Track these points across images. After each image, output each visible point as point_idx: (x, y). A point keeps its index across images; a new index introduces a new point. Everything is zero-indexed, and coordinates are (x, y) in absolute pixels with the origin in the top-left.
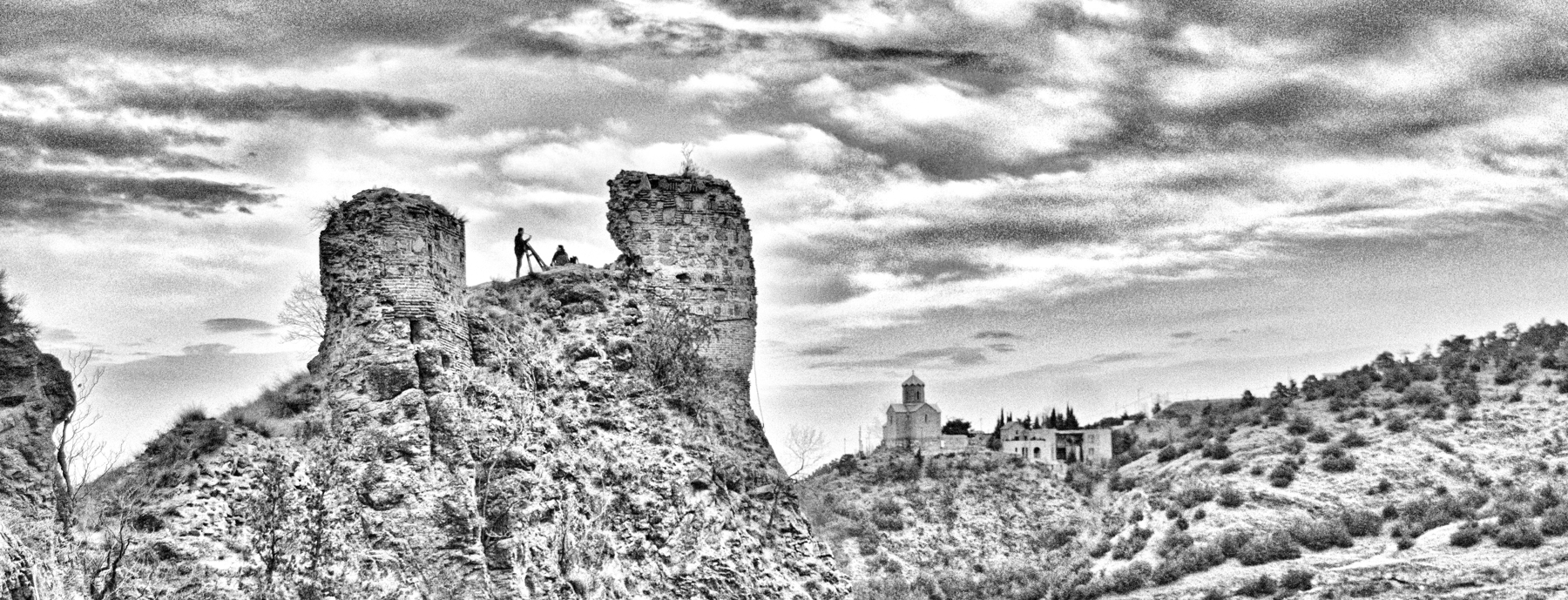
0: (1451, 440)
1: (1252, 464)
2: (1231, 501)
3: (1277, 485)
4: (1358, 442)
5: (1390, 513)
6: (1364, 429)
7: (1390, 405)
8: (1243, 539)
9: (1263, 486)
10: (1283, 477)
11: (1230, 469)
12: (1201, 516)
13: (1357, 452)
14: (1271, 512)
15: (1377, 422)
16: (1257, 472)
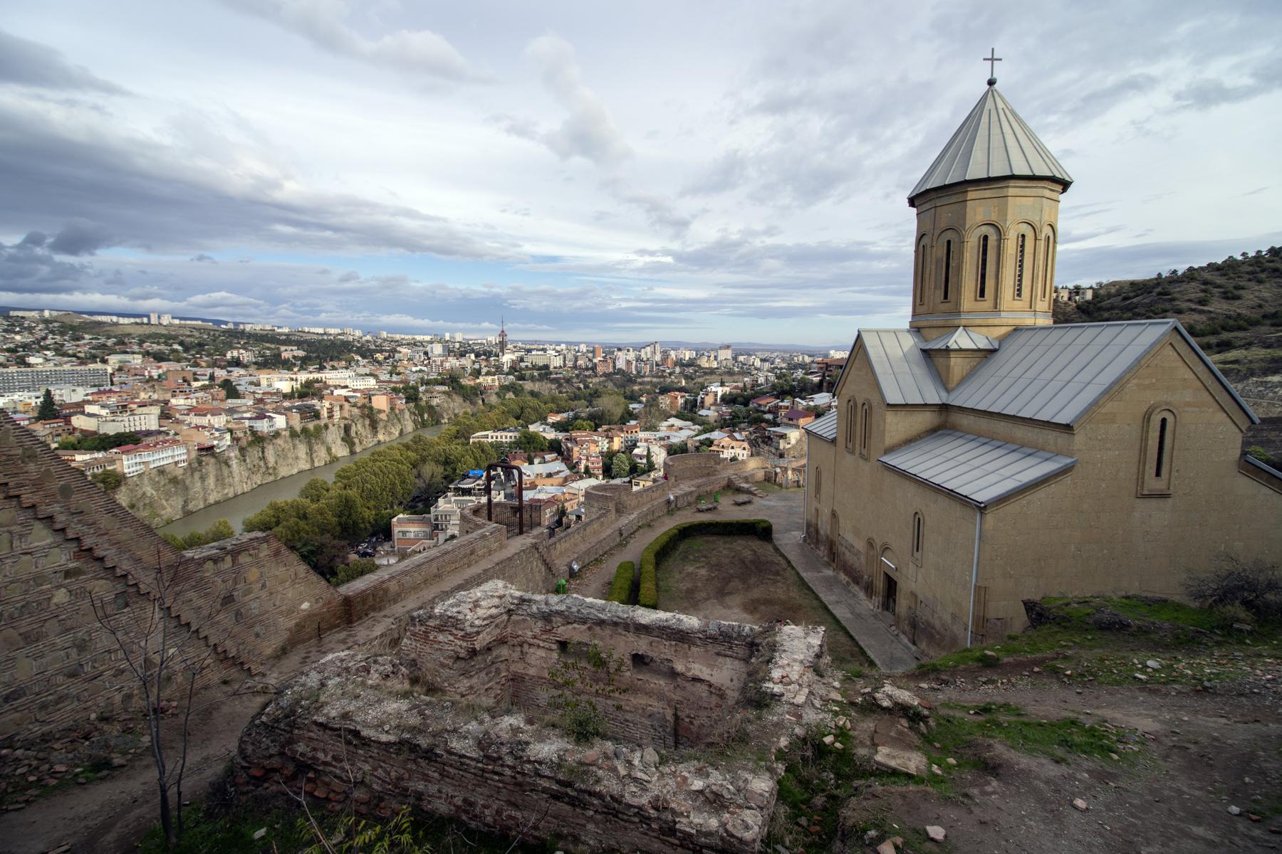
9: (1194, 306)
10: (1202, 302)
13: (1241, 292)
16: (1190, 301)
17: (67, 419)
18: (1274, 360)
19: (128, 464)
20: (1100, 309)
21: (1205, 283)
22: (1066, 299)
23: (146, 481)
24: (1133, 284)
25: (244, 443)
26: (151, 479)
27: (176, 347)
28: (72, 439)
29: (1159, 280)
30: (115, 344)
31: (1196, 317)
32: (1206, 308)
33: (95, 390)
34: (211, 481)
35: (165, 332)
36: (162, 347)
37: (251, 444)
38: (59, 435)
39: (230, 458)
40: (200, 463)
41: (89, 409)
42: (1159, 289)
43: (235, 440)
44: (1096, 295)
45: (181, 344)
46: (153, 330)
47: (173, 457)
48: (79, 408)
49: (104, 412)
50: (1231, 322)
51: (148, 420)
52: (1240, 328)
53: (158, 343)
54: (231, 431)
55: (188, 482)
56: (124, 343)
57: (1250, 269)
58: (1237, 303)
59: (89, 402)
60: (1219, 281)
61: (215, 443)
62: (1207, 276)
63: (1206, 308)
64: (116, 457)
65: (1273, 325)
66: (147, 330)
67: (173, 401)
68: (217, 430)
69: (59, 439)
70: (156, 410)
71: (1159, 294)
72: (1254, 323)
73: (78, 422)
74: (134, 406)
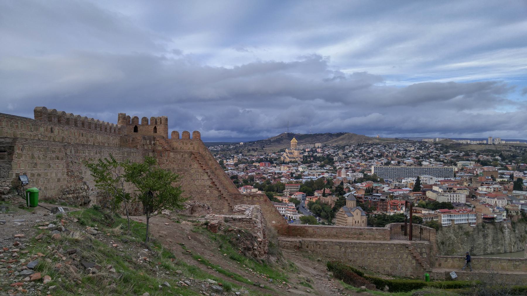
17: (424, 192)
19: (444, 219)
23: (452, 231)
25: (515, 219)
26: (454, 230)
27: (498, 157)
28: (424, 202)
30: (464, 155)
33: (443, 179)
34: (490, 240)
35: (494, 149)
36: (490, 158)
37: (520, 221)
38: (419, 200)
39: (504, 228)
40: (483, 226)
41: (435, 188)
43: (509, 216)
45: (501, 156)
46: (487, 147)
47: (468, 220)
48: (430, 188)
49: (440, 190)
51: (461, 197)
53: (487, 155)
54: (507, 210)
55: (475, 236)
56: (468, 155)
59: (435, 185)
61: (495, 216)
64: (439, 214)
66: (483, 148)
67: (480, 188)
68: (498, 208)
69: (419, 202)
70: (467, 193)
73: (429, 194)
74: (455, 189)
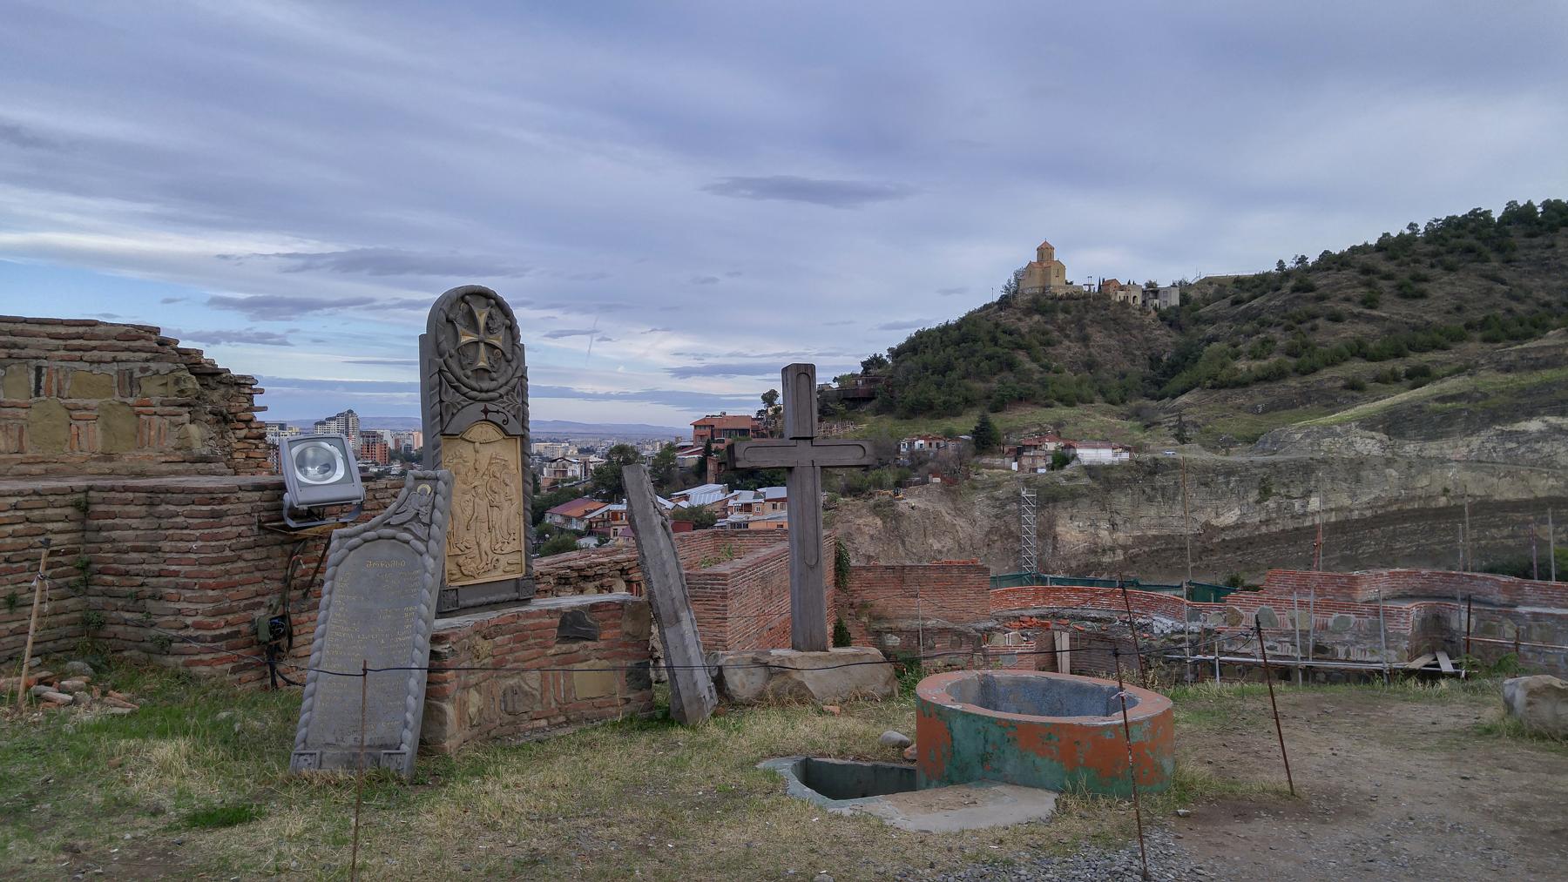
0: (1506, 274)
1: (1341, 295)
2: (1336, 318)
3: (1371, 308)
4: (1425, 280)
5: (1469, 326)
6: (1423, 270)
7: (1435, 254)
8: (1360, 344)
9: (1356, 310)
10: (1369, 302)
11: (1322, 298)
12: (1314, 329)
13: (1424, 286)
14: (1371, 327)
15: (1432, 266)
16: (1347, 300)
18: (1524, 392)
20: (1197, 321)
21: (1366, 271)
22: (1139, 301)
24: (1238, 281)
29: (1284, 274)
31: (1366, 328)
32: (1375, 313)
42: (1292, 283)
44: (1184, 299)
50: (1421, 337)
52: (1435, 346)
57: (1430, 248)
58: (1421, 303)
60: (1386, 267)
62: (1363, 258)
63: (1375, 313)
65: (1485, 340)
71: (1295, 289)
72: (1459, 338)
